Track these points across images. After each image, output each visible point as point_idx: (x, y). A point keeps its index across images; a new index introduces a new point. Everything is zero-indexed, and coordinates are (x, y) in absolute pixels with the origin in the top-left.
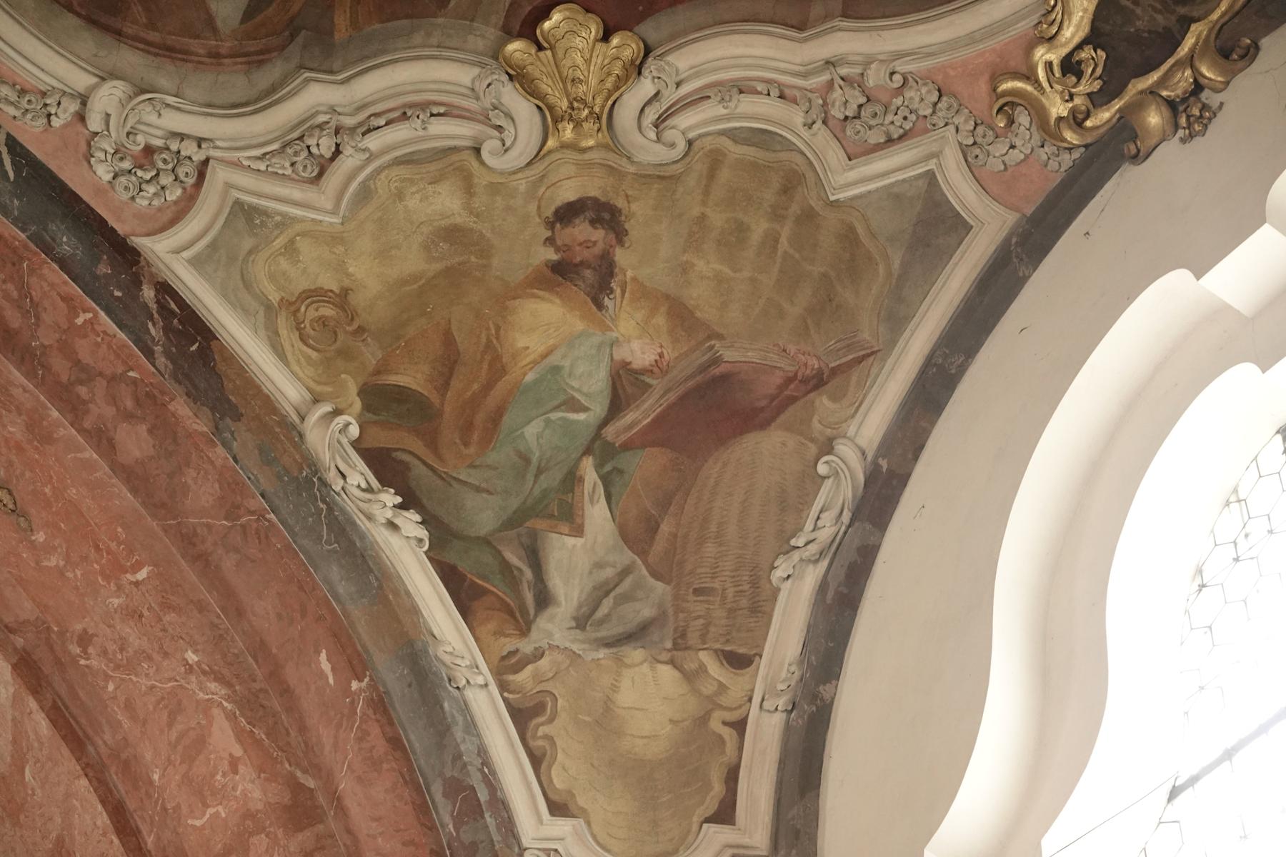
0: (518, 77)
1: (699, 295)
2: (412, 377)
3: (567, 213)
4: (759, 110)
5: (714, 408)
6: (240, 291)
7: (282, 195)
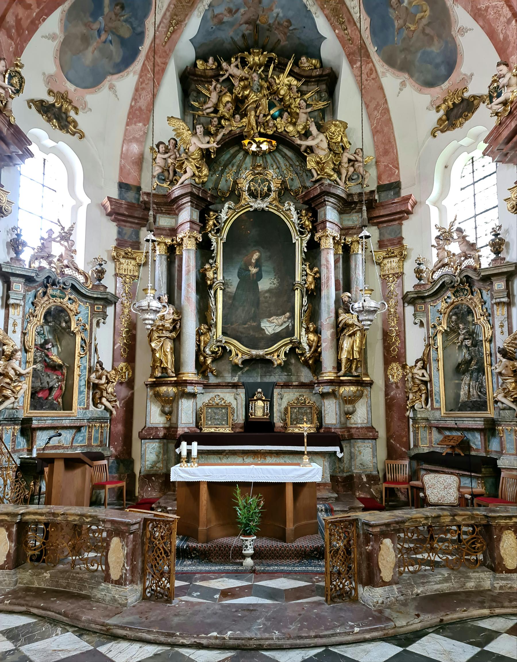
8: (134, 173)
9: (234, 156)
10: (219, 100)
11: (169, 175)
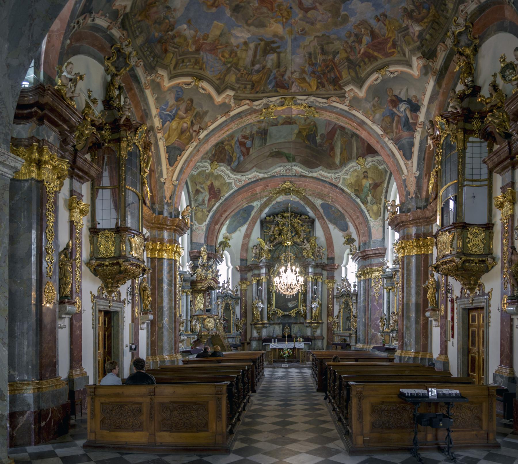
0: (358, 163)
1: (373, 177)
2: (357, 188)
3: (364, 172)
4: (374, 163)
5: (376, 186)
6: (345, 185)
7: (345, 177)
8: (245, 255)
9: (279, 247)
10: (274, 229)
11: (258, 256)
